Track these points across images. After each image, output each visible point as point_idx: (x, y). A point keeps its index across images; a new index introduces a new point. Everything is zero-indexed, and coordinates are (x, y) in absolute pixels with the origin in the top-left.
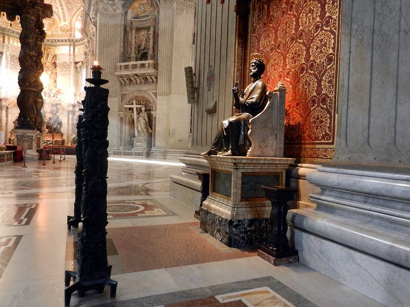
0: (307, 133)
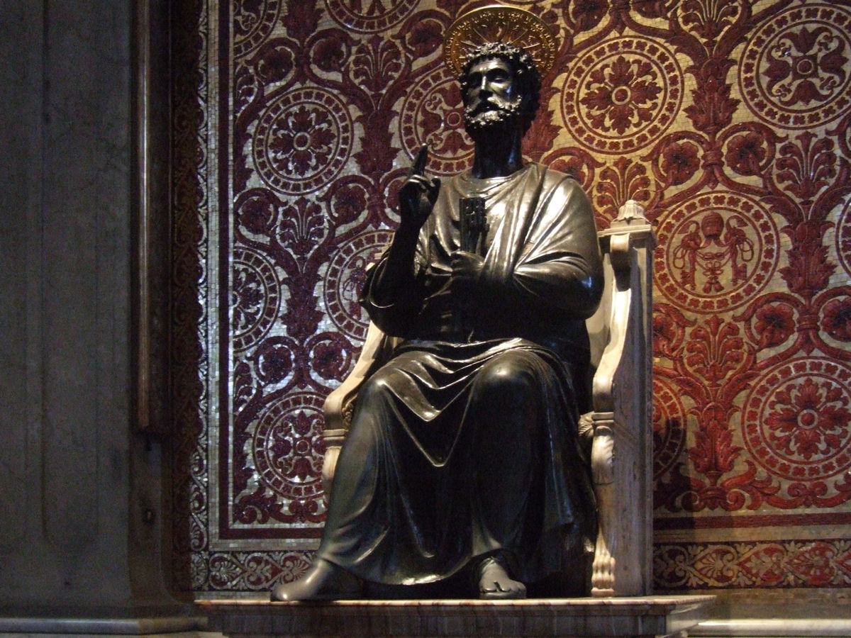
0: (741, 467)
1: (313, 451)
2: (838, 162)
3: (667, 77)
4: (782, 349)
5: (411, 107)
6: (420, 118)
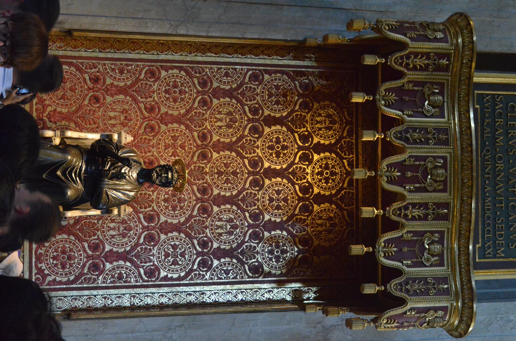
1: (63, 93)
2: (144, 264)
3: (178, 215)
4: (87, 249)
5: (181, 131)
6: (177, 135)
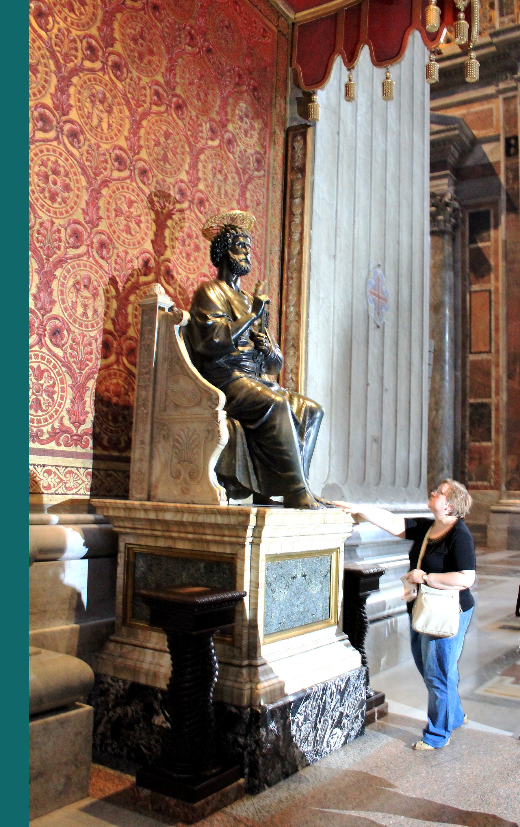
6: (114, 206)
